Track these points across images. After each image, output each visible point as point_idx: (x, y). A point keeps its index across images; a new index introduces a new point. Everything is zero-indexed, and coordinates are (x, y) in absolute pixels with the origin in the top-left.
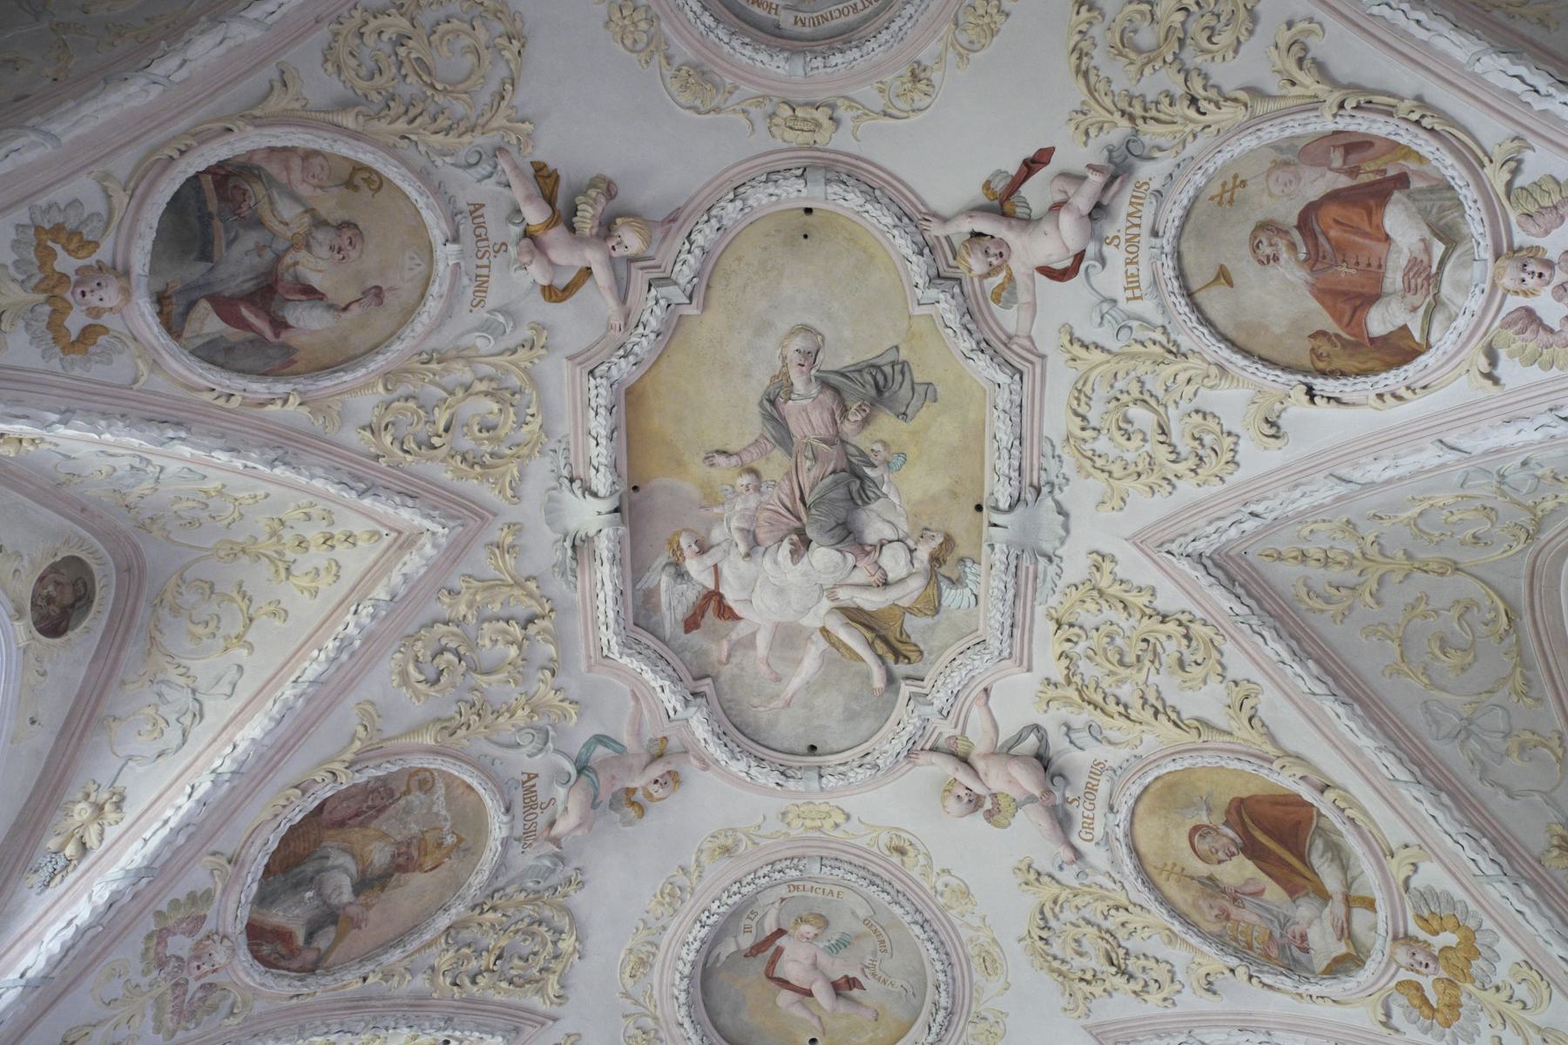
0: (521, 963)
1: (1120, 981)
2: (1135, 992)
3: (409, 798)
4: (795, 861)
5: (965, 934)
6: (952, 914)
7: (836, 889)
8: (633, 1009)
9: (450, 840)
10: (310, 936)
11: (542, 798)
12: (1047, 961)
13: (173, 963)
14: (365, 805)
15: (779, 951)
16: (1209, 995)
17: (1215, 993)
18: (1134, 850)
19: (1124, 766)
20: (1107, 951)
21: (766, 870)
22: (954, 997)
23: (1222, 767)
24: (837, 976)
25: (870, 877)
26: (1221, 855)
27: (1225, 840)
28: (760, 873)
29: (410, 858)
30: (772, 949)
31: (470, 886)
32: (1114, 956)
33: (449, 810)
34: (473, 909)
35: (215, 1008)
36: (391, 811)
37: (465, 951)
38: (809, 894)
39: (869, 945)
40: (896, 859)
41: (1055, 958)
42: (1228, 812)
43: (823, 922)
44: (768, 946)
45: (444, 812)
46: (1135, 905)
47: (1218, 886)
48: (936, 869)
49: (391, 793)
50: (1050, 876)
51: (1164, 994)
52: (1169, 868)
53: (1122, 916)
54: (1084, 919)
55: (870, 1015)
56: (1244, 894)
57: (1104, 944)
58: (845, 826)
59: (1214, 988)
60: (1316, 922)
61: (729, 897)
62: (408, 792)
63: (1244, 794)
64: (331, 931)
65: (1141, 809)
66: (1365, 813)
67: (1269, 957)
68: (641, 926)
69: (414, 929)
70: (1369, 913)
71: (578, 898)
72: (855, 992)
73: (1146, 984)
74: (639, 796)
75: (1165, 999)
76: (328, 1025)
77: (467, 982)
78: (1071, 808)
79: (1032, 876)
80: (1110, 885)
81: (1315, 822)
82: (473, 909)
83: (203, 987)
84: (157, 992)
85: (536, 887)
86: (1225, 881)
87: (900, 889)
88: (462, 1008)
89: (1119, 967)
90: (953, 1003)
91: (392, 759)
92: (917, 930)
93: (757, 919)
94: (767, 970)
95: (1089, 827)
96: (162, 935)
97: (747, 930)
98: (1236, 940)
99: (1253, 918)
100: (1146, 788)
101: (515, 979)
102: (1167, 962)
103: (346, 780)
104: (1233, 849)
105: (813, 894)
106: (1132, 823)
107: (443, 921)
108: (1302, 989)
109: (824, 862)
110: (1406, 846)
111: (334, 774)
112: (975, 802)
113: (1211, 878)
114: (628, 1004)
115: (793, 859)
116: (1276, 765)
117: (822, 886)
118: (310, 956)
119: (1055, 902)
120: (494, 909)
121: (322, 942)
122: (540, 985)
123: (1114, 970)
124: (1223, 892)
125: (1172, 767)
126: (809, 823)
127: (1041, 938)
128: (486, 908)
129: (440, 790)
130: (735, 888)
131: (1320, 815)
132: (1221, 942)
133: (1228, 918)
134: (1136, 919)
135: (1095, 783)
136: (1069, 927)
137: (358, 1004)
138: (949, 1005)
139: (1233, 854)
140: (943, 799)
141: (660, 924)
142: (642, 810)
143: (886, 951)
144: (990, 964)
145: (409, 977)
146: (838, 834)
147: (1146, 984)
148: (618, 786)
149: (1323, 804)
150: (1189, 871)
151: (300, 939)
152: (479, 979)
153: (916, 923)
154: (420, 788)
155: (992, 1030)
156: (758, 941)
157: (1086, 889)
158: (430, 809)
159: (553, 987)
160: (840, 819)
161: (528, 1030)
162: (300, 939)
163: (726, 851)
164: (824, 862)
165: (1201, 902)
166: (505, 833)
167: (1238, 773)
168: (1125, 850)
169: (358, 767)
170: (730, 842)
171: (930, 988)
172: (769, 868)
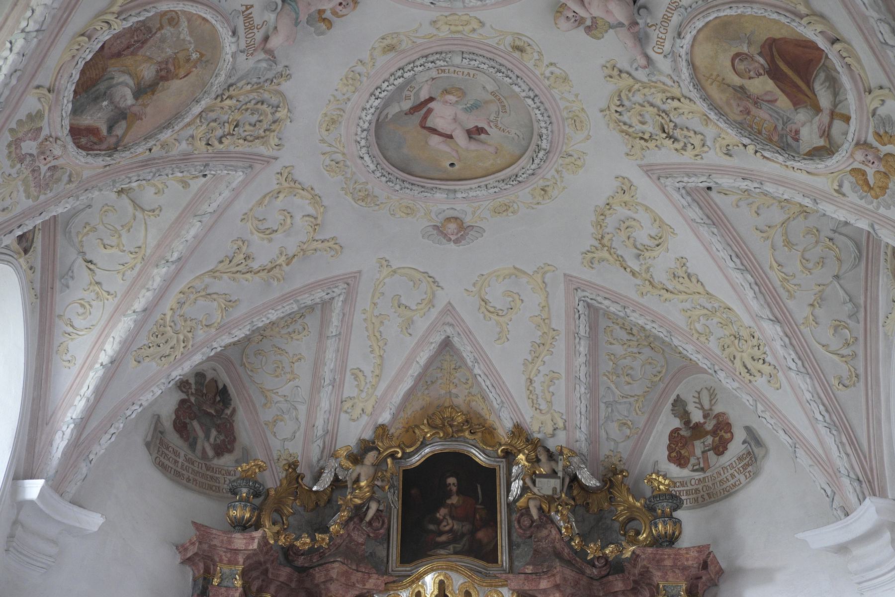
0: (252, 128)
1: (668, 142)
2: (676, 150)
3: (163, 31)
4: (443, 55)
5: (562, 104)
6: (555, 92)
7: (472, 72)
8: (328, 149)
9: (194, 56)
11: (257, 21)
12: (619, 125)
14: (133, 41)
15: (430, 111)
16: (728, 157)
17: (731, 156)
18: (692, 64)
19: (693, 6)
20: (661, 123)
21: (422, 61)
22: (551, 142)
23: (765, 16)
24: (471, 126)
25: (498, 67)
26: (752, 74)
27: (756, 65)
28: (418, 63)
29: (169, 71)
30: (425, 110)
31: (212, 85)
32: (666, 127)
33: (191, 36)
34: (216, 99)
36: (151, 42)
37: (213, 124)
38: (453, 75)
39: (493, 108)
40: (517, 54)
41: (625, 124)
42: (763, 46)
43: (462, 93)
44: (422, 107)
45: (188, 38)
46: (686, 97)
47: (746, 93)
48: (546, 62)
49: (149, 30)
50: (628, 73)
51: (696, 152)
52: (714, 77)
53: (676, 103)
54: (648, 102)
55: (492, 150)
56: (762, 100)
57: (660, 119)
58: (480, 31)
59: (730, 152)
60: (808, 124)
61: (395, 79)
62: (161, 27)
63: (778, 36)
65: (701, 36)
66: (859, 61)
67: (771, 140)
68: (332, 99)
69: (177, 116)
70: (844, 125)
71: (286, 86)
72: (483, 136)
73: (685, 145)
74: (328, 15)
75: (696, 155)
77: (216, 143)
78: (650, 31)
79: (616, 72)
80: (670, 83)
81: (823, 61)
82: (216, 99)
85: (258, 81)
86: (752, 90)
87: (519, 75)
88: (214, 157)
89: (668, 134)
90: (551, 146)
91: (147, 7)
92: (530, 101)
93: (415, 90)
94: (421, 122)
95: (661, 42)
97: (408, 98)
98: (751, 127)
99: (767, 116)
100: (708, 23)
101: (248, 138)
102: (702, 134)
103: (119, 26)
104: (762, 71)
105: (456, 75)
106: (692, 46)
107: (197, 109)
108: (789, 163)
109: (465, 56)
110: (881, 88)
111: (107, 23)
112: (580, 21)
113: (742, 87)
114: (325, 148)
115: (441, 53)
116: (804, 21)
117: (462, 70)
119: (629, 91)
120: (230, 97)
122: (265, 139)
123: (664, 135)
124: (749, 97)
125: (728, 12)
126: (453, 28)
127: (616, 111)
128: (225, 97)
129: (184, 24)
130: (399, 73)
131: (827, 57)
132: (742, 127)
133: (748, 113)
134: (685, 106)
135: (670, 15)
136: (637, 106)
138: (548, 148)
139: (761, 75)
140: (555, 18)
141: (345, 97)
142: (329, 24)
143: (506, 112)
144: (577, 122)
145: (177, 144)
146: (475, 36)
147: (685, 145)
148: (313, 9)
149: (832, 53)
150: (728, 81)
152: (224, 140)
153: (529, 97)
154: (170, 24)
155: (576, 163)
156: (415, 105)
157: (653, 84)
158: (178, 38)
159: (273, 141)
160: (475, 25)
161: (258, 166)
163: (391, 48)
164: (465, 56)
165: (732, 101)
166: (234, 48)
167: (776, 22)
168: (684, 63)
169: (123, 16)
170: (395, 41)
171: (535, 137)
172: (424, 59)
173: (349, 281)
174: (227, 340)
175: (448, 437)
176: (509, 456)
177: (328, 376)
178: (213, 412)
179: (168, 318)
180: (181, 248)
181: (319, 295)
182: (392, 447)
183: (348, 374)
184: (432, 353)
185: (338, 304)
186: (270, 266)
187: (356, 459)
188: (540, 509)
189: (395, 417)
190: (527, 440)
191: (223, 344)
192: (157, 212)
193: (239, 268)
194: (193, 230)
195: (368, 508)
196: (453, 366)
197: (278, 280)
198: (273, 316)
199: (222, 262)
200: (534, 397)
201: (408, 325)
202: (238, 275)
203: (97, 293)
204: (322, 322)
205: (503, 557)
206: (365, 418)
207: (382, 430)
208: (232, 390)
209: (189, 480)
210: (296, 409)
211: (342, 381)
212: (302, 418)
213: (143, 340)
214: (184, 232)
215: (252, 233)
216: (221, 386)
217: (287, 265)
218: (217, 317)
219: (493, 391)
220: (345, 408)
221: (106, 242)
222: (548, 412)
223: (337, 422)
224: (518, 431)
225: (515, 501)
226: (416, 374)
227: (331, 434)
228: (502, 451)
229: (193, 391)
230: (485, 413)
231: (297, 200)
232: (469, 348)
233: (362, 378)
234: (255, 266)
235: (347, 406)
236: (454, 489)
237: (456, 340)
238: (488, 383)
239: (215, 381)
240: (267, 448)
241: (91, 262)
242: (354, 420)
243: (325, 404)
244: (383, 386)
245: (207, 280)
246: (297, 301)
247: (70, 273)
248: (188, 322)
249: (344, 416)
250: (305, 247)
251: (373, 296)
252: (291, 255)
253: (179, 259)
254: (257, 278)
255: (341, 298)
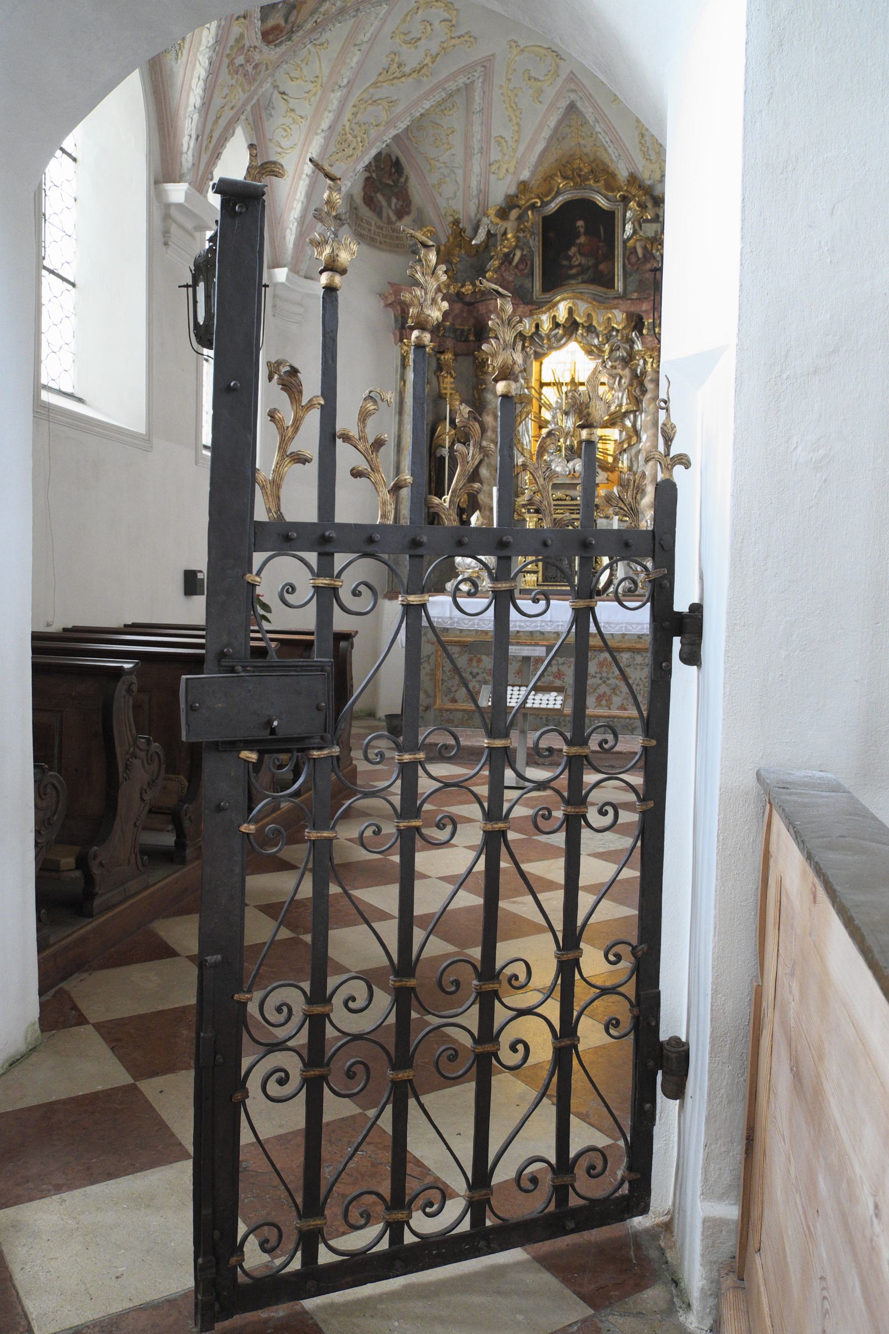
10: (286, 21)
13: (241, 69)
35: (260, 71)
64: (295, 12)
76: (304, 43)
83: (253, 68)
84: (239, 83)
96: (232, 63)
118: (289, 26)
121: (292, 18)
137: (313, 30)
151: (283, 23)
162: (283, 23)
173: (486, 64)
174: (393, 132)
175: (577, 186)
176: (625, 200)
177: (476, 146)
178: (391, 183)
179: (347, 128)
180: (348, 74)
181: (462, 80)
182: (532, 199)
183: (493, 141)
184: (560, 117)
185: (478, 85)
186: (419, 67)
187: (503, 214)
188: (645, 248)
189: (533, 173)
190: (640, 187)
191: (391, 136)
192: (325, 45)
193: (395, 75)
194: (355, 58)
195: (514, 255)
196: (579, 123)
197: (427, 76)
198: (427, 105)
199: (380, 74)
200: (645, 149)
201: (540, 91)
202: (395, 81)
203: (293, 119)
204: (467, 100)
205: (619, 285)
206: (509, 177)
207: (524, 186)
208: (403, 160)
209: (381, 243)
210: (455, 173)
211: (489, 149)
212: (460, 179)
213: (332, 149)
214: (348, 61)
215: (401, 46)
216: (394, 159)
217: (433, 62)
218: (384, 117)
219: (611, 145)
220: (493, 170)
221: (292, 75)
222: (656, 162)
223: (487, 183)
224: (633, 179)
225: (629, 239)
226: (547, 136)
227: (484, 193)
228: (620, 196)
229: (374, 168)
230: (607, 161)
231: (434, 10)
232: (591, 110)
233: (504, 144)
234: (407, 70)
235: (493, 168)
236: (582, 230)
237: (579, 104)
238: (607, 139)
239: (389, 155)
240: (436, 206)
241: (284, 93)
242: (500, 179)
243: (476, 169)
244: (521, 148)
245: (371, 90)
246: (444, 89)
247: (271, 104)
248: (363, 127)
249: (492, 177)
250: (445, 45)
251: (507, 73)
252: (434, 54)
253: (348, 83)
254: (410, 79)
255: (480, 80)
